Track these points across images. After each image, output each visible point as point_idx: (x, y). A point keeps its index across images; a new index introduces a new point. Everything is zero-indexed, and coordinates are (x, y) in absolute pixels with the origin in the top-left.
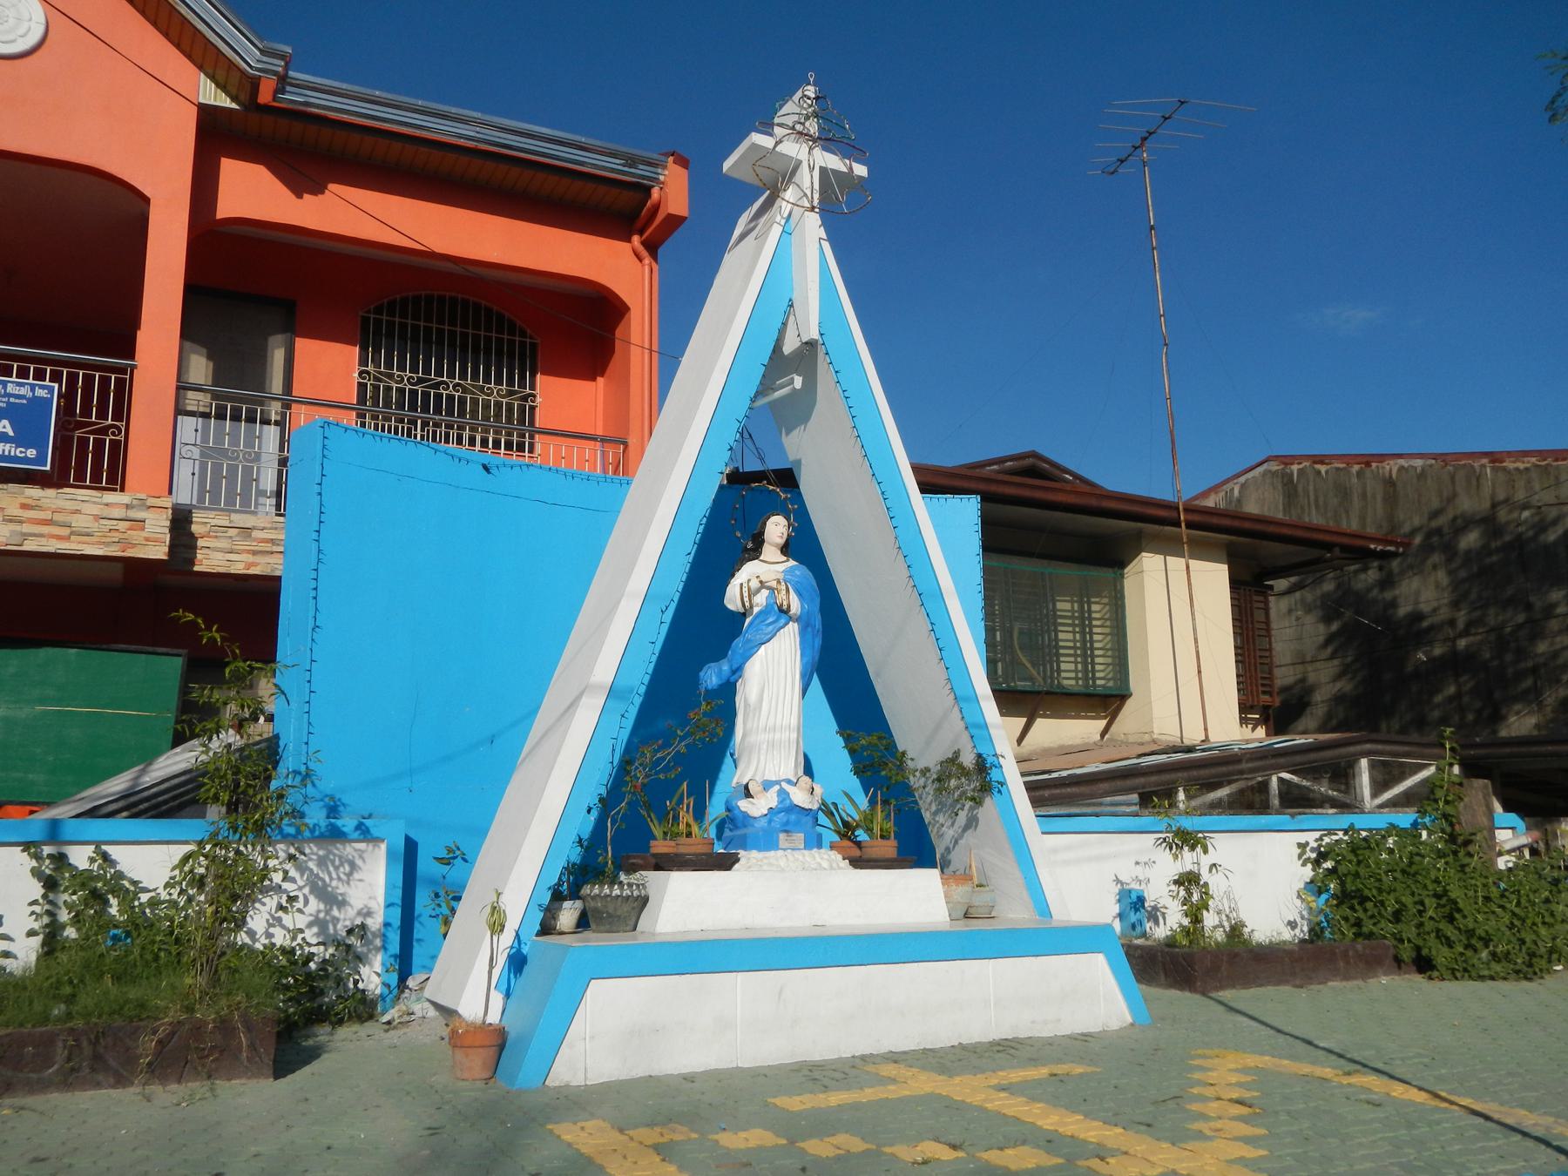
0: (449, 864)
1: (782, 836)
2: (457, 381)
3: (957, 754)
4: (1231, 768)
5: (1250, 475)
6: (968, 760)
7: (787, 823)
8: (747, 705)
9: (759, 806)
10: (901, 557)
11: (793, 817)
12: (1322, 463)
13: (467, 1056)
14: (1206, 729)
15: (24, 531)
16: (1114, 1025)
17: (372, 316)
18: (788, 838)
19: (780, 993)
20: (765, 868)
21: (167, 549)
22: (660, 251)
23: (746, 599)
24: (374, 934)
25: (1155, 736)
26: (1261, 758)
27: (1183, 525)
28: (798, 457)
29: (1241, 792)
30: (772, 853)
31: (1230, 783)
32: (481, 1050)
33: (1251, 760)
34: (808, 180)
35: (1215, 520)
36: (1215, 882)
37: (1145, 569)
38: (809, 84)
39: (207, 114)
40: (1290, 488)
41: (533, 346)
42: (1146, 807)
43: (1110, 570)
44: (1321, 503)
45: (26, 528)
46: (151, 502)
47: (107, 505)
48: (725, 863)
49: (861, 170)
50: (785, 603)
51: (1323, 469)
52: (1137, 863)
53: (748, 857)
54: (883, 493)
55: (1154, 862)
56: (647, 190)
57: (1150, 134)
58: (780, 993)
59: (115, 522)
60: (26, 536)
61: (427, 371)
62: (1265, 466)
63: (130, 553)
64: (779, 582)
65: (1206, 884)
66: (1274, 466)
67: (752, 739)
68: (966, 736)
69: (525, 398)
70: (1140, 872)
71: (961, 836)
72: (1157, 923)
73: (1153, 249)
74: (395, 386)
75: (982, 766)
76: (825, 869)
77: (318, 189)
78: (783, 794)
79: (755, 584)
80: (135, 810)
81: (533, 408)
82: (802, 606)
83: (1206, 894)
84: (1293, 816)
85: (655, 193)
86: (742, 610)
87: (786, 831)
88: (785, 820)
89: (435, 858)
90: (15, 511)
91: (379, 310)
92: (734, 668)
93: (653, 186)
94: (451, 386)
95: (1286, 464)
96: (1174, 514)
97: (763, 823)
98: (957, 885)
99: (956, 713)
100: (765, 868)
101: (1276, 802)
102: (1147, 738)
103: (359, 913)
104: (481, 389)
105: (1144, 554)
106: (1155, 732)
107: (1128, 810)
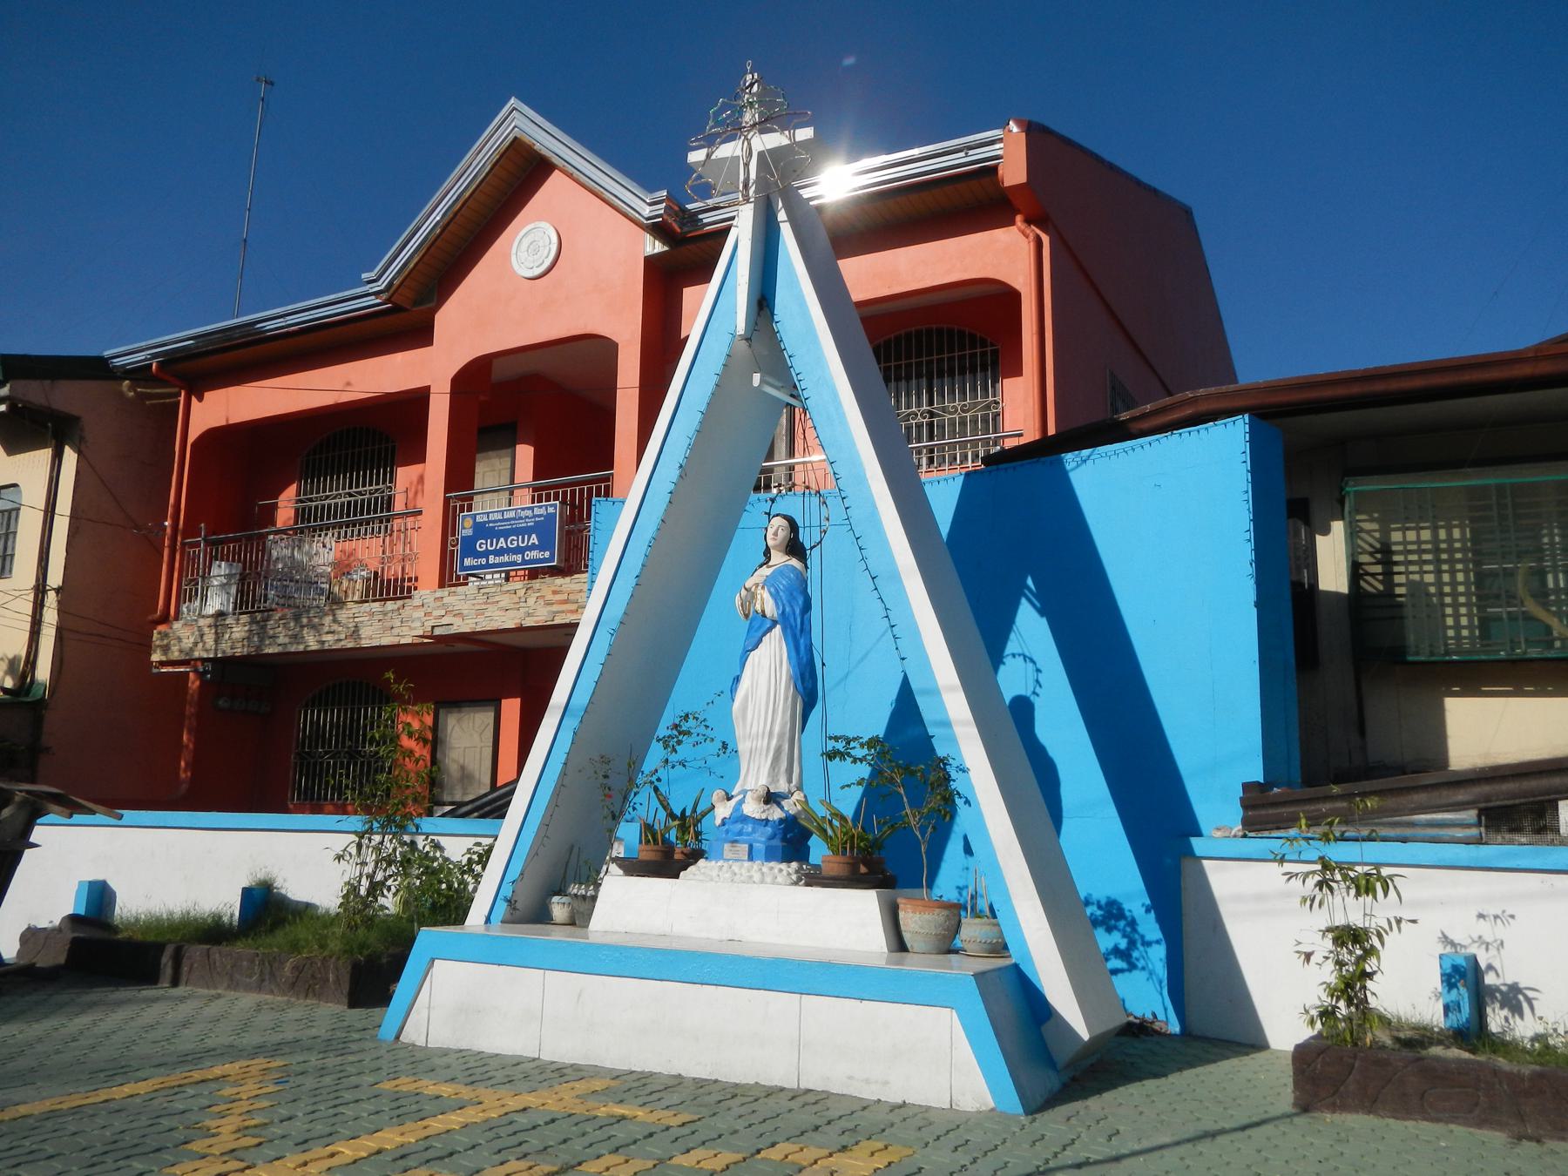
1: (727, 846)
15: (555, 610)
18: (733, 849)
19: (579, 995)
39: (649, 261)
42: (1498, 831)
45: (555, 608)
52: (1481, 916)
55: (1512, 917)
58: (579, 995)
70: (1486, 929)
72: (1517, 1010)
76: (754, 882)
80: (482, 812)
90: (550, 597)
98: (914, 912)
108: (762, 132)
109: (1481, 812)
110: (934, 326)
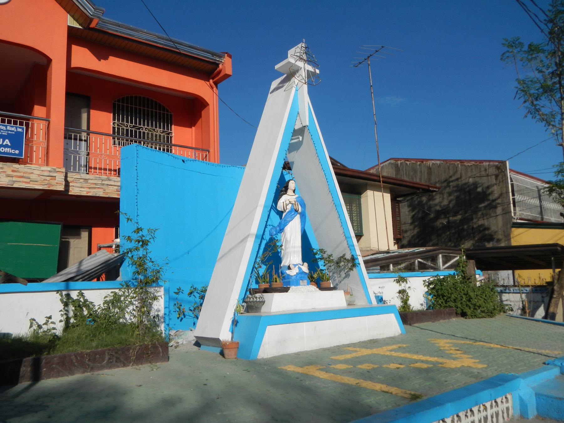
0: (178, 294)
1: (301, 281)
2: (146, 127)
3: (344, 255)
4: (405, 258)
5: (384, 164)
6: (348, 257)
7: (301, 277)
8: (286, 240)
9: (293, 272)
10: (330, 194)
11: (303, 275)
12: (408, 161)
13: (230, 351)
14: (388, 246)
15: (14, 180)
16: (397, 334)
17: (117, 103)
19: (315, 328)
20: (298, 291)
21: (64, 187)
22: (219, 85)
23: (285, 207)
24: (161, 317)
25: (371, 248)
26: (412, 255)
27: (381, 182)
28: (292, 161)
29: (408, 265)
30: (299, 287)
31: (405, 262)
32: (234, 349)
33: (410, 255)
34: (303, 73)
35: (389, 180)
36: (410, 293)
37: (368, 195)
38: (303, 43)
39: (71, 29)
40: (397, 168)
41: (171, 115)
43: (357, 195)
44: (407, 173)
45: (14, 179)
46: (58, 170)
47: (42, 171)
48: (286, 290)
49: (318, 71)
50: (297, 208)
51: (408, 163)
52: (379, 287)
53: (293, 288)
54: (325, 174)
56: (218, 65)
57: (371, 55)
58: (315, 328)
59: (45, 177)
60: (14, 182)
61: (136, 123)
62: (389, 161)
63: (51, 188)
64: (295, 202)
65: (407, 293)
66: (392, 161)
67: (288, 250)
68: (348, 249)
69: (168, 134)
70: (380, 290)
71: (343, 280)
73: (372, 93)
74: (125, 128)
75: (353, 259)
77: (106, 58)
78: (300, 268)
79: (288, 202)
80: (84, 279)
81: (171, 137)
82: (302, 209)
83: (407, 296)
84: (422, 272)
85: (221, 66)
86: (283, 210)
87: (302, 280)
88: (301, 276)
89: (174, 292)
90: (10, 172)
91: (119, 101)
92: (281, 228)
93: (220, 64)
94: (145, 129)
95: (396, 161)
96: (379, 178)
97: (294, 277)
99: (345, 242)
100: (298, 291)
101: (417, 268)
102: (369, 249)
103: (156, 311)
104: (154, 130)
105: (368, 191)
106: (371, 246)
107: (377, 271)
108: (308, 64)
109: (380, 267)
110: (134, 95)
